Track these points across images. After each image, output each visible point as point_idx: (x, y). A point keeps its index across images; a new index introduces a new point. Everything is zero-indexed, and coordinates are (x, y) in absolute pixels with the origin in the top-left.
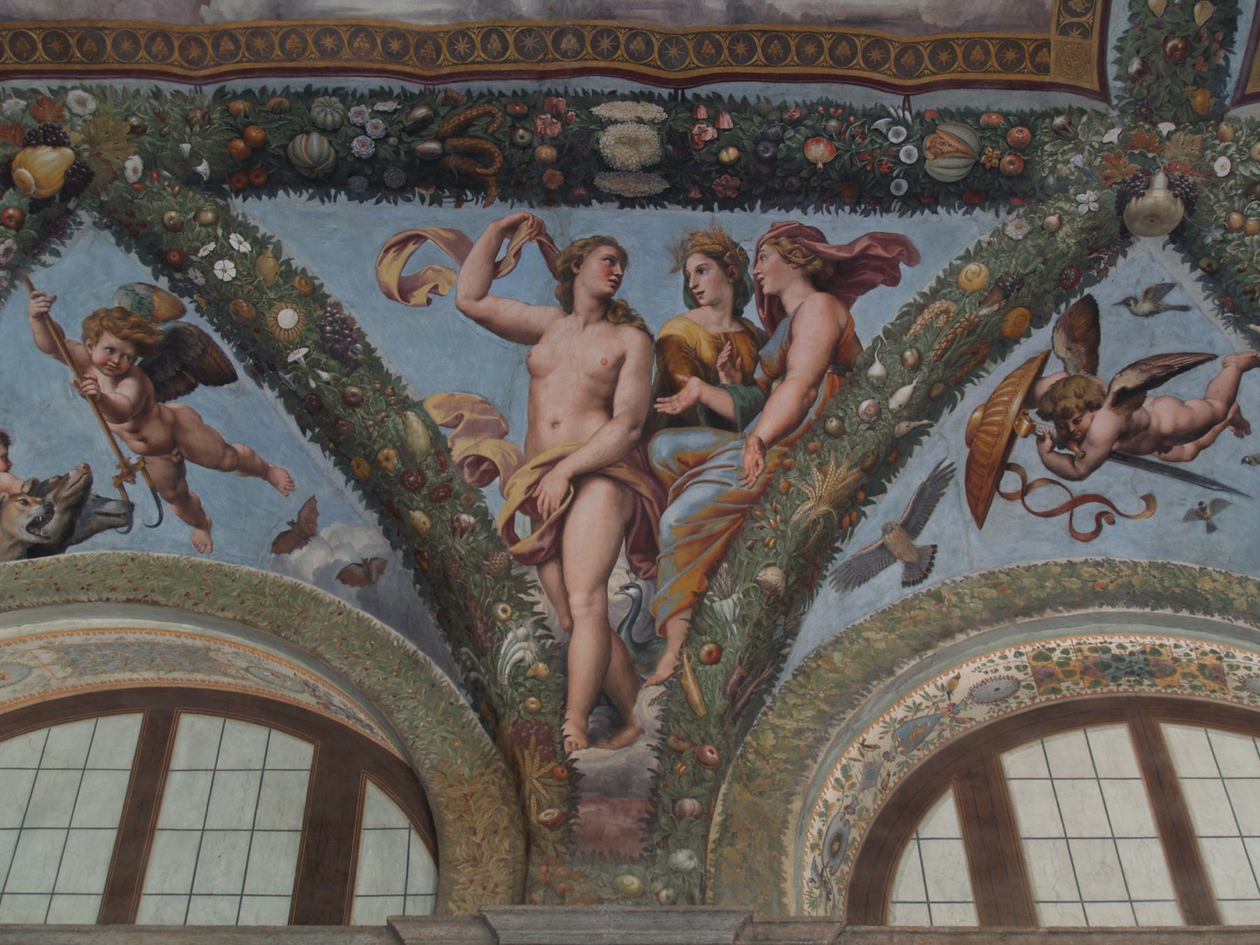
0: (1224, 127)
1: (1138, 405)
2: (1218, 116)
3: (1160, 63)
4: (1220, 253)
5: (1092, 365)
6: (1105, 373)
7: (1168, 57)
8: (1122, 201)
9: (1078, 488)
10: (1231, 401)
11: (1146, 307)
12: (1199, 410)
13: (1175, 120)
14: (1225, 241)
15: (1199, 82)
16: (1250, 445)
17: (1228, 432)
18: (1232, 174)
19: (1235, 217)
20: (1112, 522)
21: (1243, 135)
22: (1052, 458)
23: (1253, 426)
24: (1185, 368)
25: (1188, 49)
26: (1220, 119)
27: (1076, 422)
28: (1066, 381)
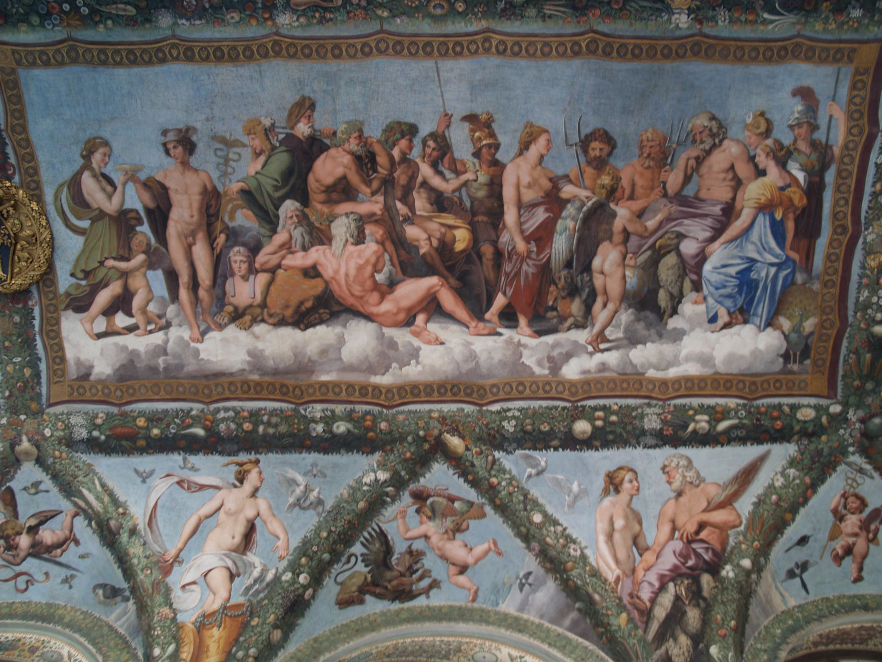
0: (45, 417)
1: (37, 533)
2: (41, 412)
3: (16, 392)
4: (55, 467)
5: (16, 515)
6: (22, 519)
7: (19, 389)
8: (12, 446)
9: (18, 569)
10: (71, 531)
11: (33, 491)
12: (61, 535)
13: (25, 414)
14: (54, 463)
15: (32, 399)
16: (81, 550)
17: (72, 544)
18: (52, 436)
19: (57, 453)
20: (33, 584)
21: (53, 419)
22: (4, 555)
23: (81, 541)
24: (52, 517)
25: (25, 387)
26: (43, 414)
27: (13, 540)
28: (7, 522)
